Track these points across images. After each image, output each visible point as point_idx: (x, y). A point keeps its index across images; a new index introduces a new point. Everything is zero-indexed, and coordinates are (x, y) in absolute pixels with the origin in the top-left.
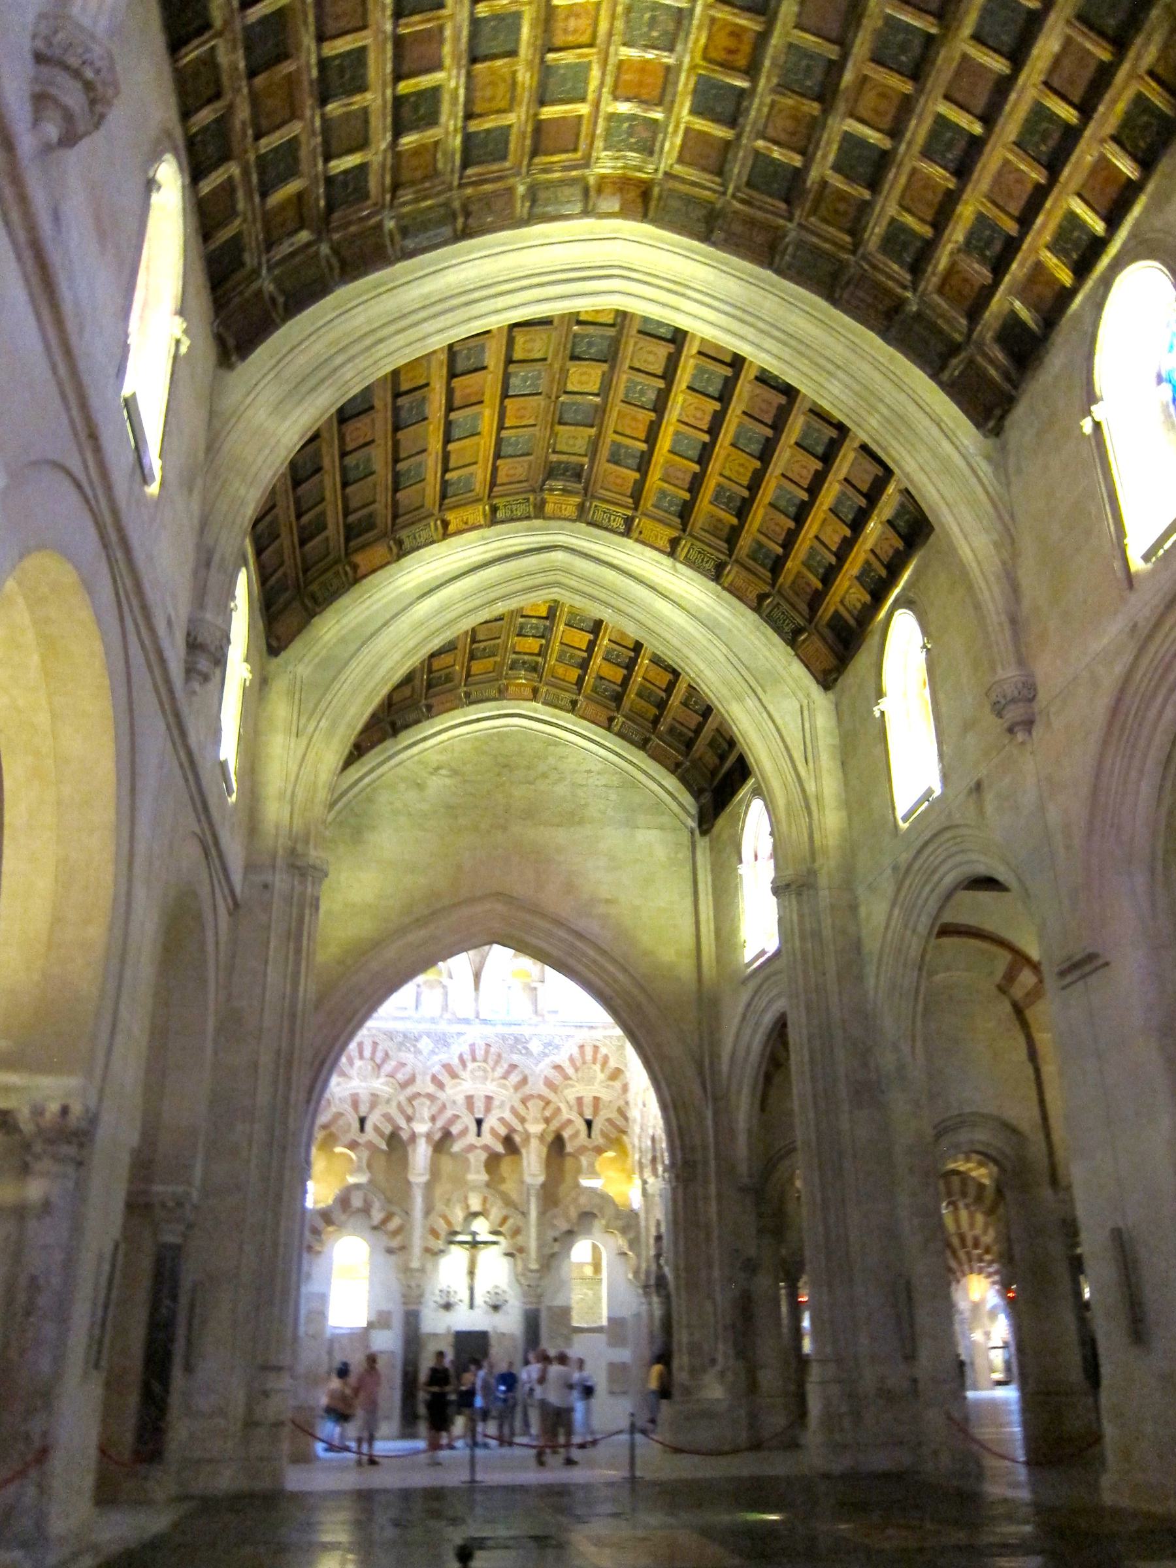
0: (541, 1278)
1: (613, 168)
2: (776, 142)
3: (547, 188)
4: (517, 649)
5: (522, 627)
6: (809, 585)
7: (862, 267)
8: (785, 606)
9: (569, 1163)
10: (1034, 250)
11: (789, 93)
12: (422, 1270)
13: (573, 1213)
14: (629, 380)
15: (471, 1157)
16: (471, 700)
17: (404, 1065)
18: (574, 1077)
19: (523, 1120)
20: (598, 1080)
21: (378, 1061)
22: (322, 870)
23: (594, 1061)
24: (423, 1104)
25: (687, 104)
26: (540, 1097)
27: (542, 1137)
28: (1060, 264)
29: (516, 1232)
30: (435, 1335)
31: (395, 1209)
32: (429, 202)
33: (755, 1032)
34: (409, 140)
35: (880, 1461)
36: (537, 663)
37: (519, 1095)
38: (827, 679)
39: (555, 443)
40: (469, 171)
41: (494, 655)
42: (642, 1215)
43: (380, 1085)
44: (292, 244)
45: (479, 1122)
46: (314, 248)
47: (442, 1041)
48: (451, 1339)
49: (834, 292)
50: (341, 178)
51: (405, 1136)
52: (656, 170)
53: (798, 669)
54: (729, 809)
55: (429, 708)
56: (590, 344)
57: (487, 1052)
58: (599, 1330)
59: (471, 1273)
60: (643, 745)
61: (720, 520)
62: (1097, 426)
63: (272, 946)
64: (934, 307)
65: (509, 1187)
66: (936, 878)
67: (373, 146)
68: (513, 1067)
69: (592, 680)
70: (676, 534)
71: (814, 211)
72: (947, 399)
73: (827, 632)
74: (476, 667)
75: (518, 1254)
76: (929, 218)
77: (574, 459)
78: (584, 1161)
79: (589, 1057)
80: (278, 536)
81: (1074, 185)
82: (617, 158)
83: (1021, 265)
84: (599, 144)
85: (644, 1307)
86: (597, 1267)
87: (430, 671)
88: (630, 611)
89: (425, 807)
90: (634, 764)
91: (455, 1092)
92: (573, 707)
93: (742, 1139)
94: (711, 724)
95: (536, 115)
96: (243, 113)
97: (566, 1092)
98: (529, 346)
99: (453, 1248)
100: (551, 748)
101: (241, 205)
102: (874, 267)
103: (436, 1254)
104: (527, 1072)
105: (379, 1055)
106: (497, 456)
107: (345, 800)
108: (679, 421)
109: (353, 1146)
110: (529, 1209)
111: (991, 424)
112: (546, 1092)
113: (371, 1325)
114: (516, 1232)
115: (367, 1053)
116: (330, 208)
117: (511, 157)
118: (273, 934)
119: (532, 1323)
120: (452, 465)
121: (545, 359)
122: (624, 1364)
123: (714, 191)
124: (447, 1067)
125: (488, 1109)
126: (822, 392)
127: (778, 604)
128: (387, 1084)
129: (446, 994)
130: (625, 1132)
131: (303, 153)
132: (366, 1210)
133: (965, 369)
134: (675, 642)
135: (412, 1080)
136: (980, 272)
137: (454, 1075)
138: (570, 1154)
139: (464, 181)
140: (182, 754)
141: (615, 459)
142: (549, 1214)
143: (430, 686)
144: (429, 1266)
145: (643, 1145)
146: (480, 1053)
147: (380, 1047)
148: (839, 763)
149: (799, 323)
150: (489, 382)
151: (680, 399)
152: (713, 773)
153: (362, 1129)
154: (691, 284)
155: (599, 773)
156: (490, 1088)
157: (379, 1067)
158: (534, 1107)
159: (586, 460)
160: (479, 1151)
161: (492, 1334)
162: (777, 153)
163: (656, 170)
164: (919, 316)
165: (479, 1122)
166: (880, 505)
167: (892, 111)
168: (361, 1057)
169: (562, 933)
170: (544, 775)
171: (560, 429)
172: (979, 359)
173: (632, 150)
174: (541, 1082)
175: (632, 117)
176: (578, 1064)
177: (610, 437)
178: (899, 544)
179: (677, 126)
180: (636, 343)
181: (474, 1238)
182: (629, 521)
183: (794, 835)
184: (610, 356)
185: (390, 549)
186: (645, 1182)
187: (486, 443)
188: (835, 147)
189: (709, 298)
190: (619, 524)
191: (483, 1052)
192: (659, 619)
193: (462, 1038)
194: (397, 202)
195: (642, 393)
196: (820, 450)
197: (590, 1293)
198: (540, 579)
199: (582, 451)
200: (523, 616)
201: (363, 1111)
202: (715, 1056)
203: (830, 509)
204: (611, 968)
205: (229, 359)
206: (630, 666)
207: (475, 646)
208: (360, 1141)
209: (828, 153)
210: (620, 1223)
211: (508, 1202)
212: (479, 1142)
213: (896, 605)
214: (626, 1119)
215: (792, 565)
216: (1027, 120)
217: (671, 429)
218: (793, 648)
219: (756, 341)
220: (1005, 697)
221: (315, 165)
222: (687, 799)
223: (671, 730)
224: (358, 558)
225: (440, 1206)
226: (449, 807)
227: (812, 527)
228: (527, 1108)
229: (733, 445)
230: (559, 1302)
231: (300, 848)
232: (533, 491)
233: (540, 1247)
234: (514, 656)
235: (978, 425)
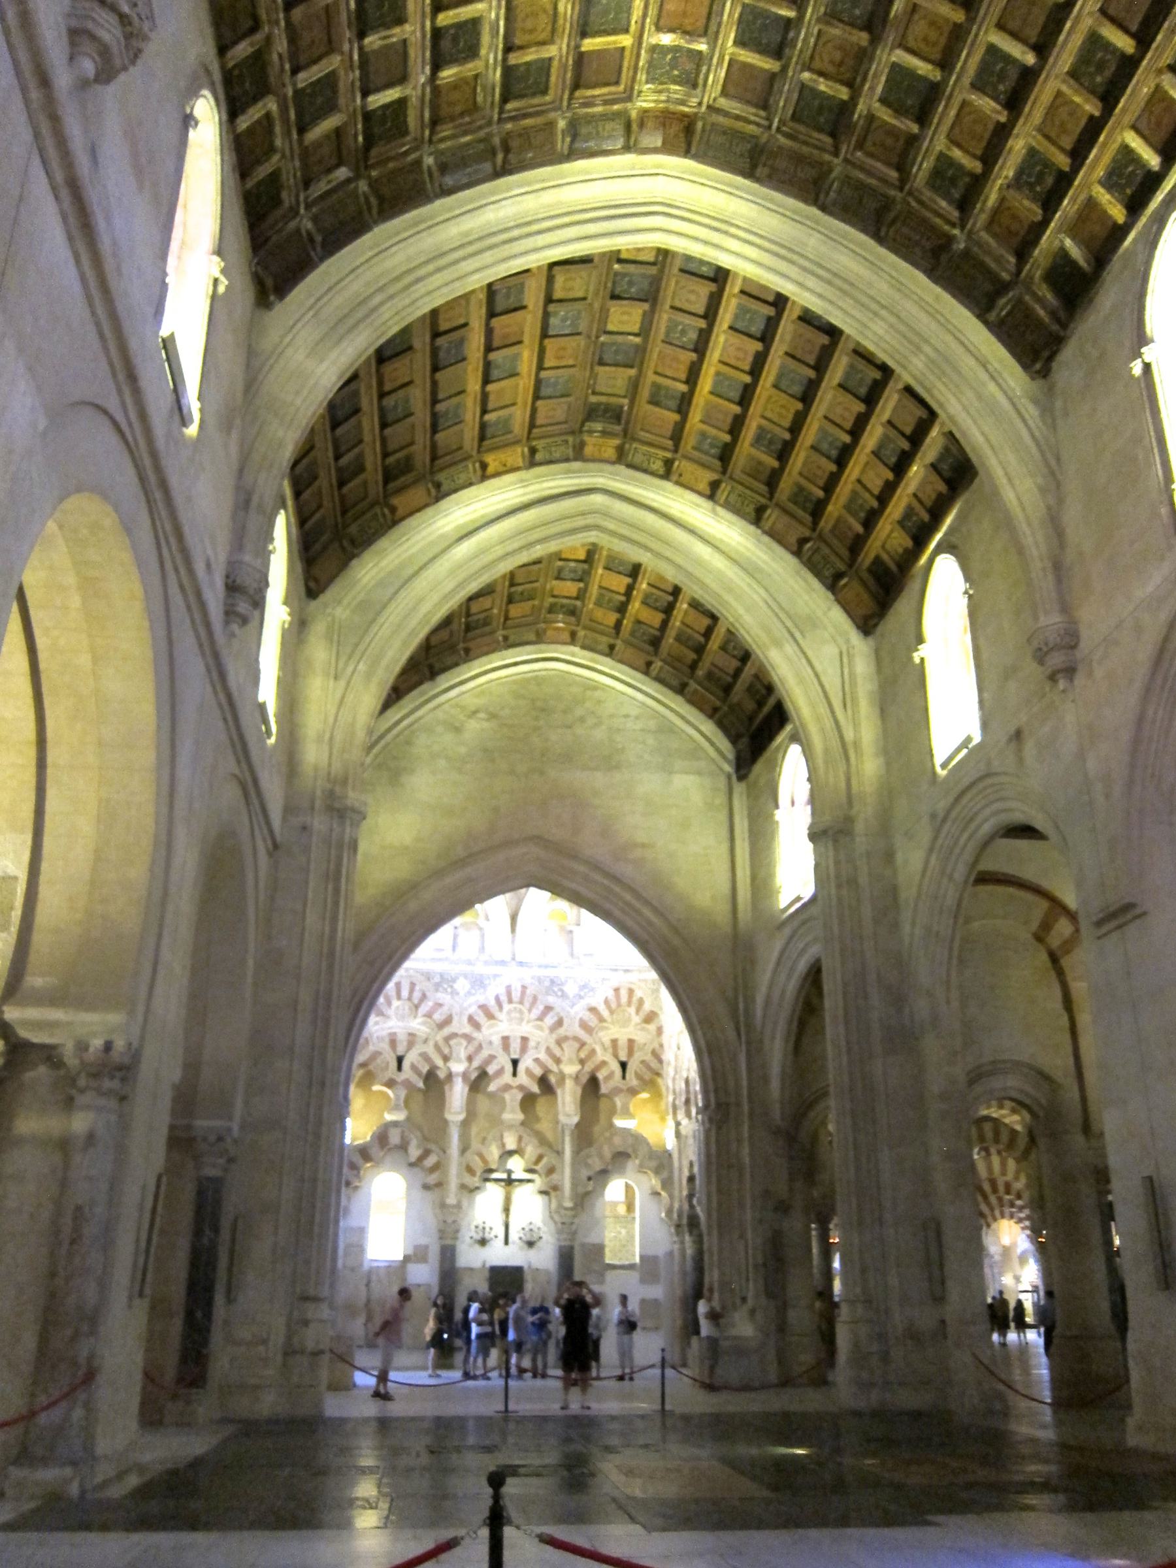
0: (575, 1216)
1: (655, 101)
2: (821, 74)
3: (589, 122)
4: (556, 593)
5: (560, 570)
6: (850, 528)
7: (908, 204)
8: (826, 550)
9: (603, 1104)
10: (1086, 185)
11: (835, 22)
12: (459, 1206)
13: (607, 1153)
14: (670, 320)
15: (507, 1096)
16: (508, 644)
17: (441, 1005)
18: (609, 1020)
19: (558, 1061)
20: (633, 1023)
21: (416, 1001)
22: (360, 812)
23: (629, 1003)
24: (461, 1044)
25: (732, 35)
26: (576, 1039)
27: (577, 1078)
28: (1113, 200)
29: (551, 1171)
30: (471, 1269)
31: (433, 1147)
32: (468, 138)
33: (789, 977)
34: (448, 74)
35: (908, 1399)
36: (575, 607)
37: (554, 1036)
38: (867, 625)
39: (595, 383)
40: (509, 106)
41: (533, 599)
42: (675, 1156)
43: (418, 1025)
44: (329, 182)
45: (515, 1063)
46: (352, 186)
47: (479, 982)
48: (487, 1274)
49: (879, 230)
50: (380, 113)
51: (442, 1074)
52: (700, 104)
53: (837, 615)
54: (767, 754)
55: (467, 651)
56: (631, 283)
57: (523, 993)
58: (631, 1267)
59: (507, 1210)
60: (680, 690)
61: (760, 463)
62: (1147, 367)
63: (312, 884)
64: (980, 244)
65: (544, 1126)
66: (973, 826)
67: (412, 82)
68: (548, 1009)
69: (630, 625)
70: (715, 476)
71: (860, 145)
72: (993, 339)
73: (865, 575)
74: (515, 611)
75: (553, 1194)
76: (979, 152)
77: (613, 400)
78: (618, 1101)
79: (624, 1000)
80: (315, 478)
81: (1128, 119)
82: (660, 92)
83: (1074, 200)
84: (642, 76)
85: (676, 1246)
86: (630, 1207)
87: (468, 615)
88: (668, 554)
89: (463, 750)
90: (672, 710)
91: (492, 1033)
92: (610, 652)
93: (775, 1084)
94: (749, 671)
95: (578, 46)
96: (281, 45)
97: (601, 1034)
98: (570, 284)
99: (488, 1184)
100: (589, 693)
101: (278, 142)
102: (920, 202)
103: (473, 1190)
104: (562, 1014)
105: (417, 995)
106: (537, 397)
107: (383, 743)
108: (720, 362)
109: (390, 1084)
110: (563, 1148)
111: (1038, 366)
112: (582, 1034)
113: (407, 1259)
114: (551, 1171)
115: (405, 993)
116: (370, 141)
117: (551, 92)
118: (312, 876)
119: (566, 1258)
120: (491, 406)
121: (584, 299)
122: (656, 1300)
123: (758, 124)
124: (484, 1008)
126: (867, 332)
127: (818, 548)
128: (424, 1023)
129: (483, 936)
130: (658, 1074)
131: (342, 86)
132: (403, 1147)
133: (1013, 308)
134: (714, 586)
135: (448, 1021)
136: (1030, 209)
137: (490, 1016)
138: (604, 1095)
139: (504, 116)
140: (222, 696)
141: (654, 401)
142: (583, 1153)
143: (468, 628)
144: (465, 1204)
145: (677, 1088)
146: (516, 995)
147: (417, 988)
148: (878, 711)
149: (845, 262)
150: (529, 322)
151: (722, 339)
152: (751, 719)
153: (400, 1068)
154: (734, 221)
155: (637, 718)
156: (526, 1029)
157: (417, 1007)
158: (569, 1049)
159: (626, 401)
160: (515, 1091)
161: (526, 1267)
162: (823, 86)
163: (700, 104)
164: (966, 254)
165: (515, 1063)
166: (923, 448)
167: (943, 41)
168: (399, 997)
169: (598, 877)
170: (582, 719)
171: (601, 370)
172: (1027, 298)
173: (675, 83)
174: (577, 1025)
175: (676, 49)
176: (614, 1006)
177: (650, 377)
178: (942, 487)
179: (721, 58)
180: (677, 282)
181: (509, 1176)
182: (668, 464)
183: (831, 780)
184: (651, 296)
185: (428, 491)
186: (678, 1124)
187: (525, 383)
188: (883, 79)
189: (752, 236)
190: (658, 466)
191: (519, 994)
192: (699, 562)
194: (435, 138)
195: (683, 332)
196: (863, 391)
197: (624, 1231)
198: (580, 522)
199: (622, 393)
200: (561, 560)
201: (400, 1050)
202: (749, 1000)
203: (873, 452)
204: (647, 912)
205: (268, 297)
206: (669, 610)
207: (513, 589)
209: (877, 84)
210: (653, 1164)
211: (543, 1141)
212: (515, 1082)
213: (939, 550)
214: (660, 1061)
215: (834, 509)
216: (1081, 49)
217: (712, 371)
218: (833, 593)
219: (801, 280)
220: (1046, 644)
221: (354, 101)
222: (725, 744)
223: (710, 676)
224: (395, 501)
225: (475, 1145)
226: (485, 750)
227: (853, 470)
228: (562, 1049)
229: (776, 386)
230: (593, 1239)
231: (338, 789)
232: (573, 433)
233: (574, 1185)
234: (551, 600)
235: (1025, 367)
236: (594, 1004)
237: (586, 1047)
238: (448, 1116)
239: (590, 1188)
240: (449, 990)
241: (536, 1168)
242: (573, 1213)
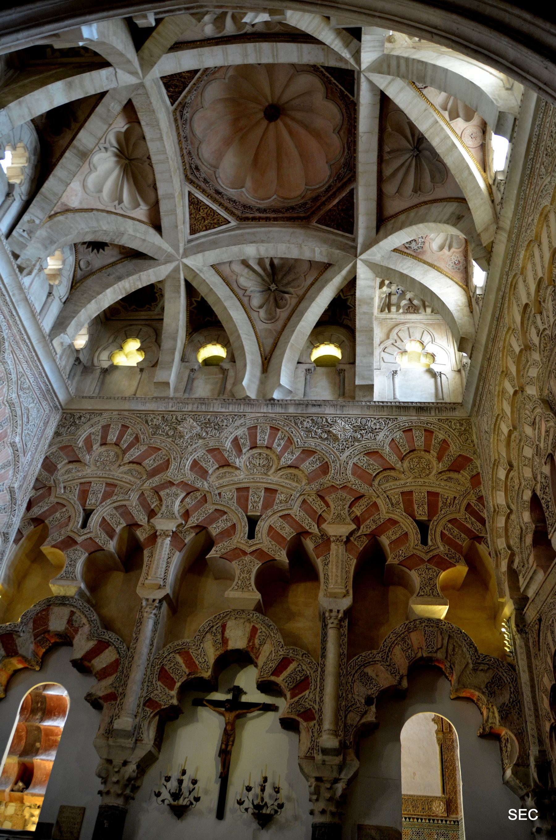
0: (341, 768)
18: (398, 466)
19: (320, 520)
20: (434, 472)
21: (125, 446)
37: (315, 486)
42: (522, 664)
45: (253, 522)
51: (141, 535)
57: (272, 437)
68: (308, 452)
105: (128, 439)
110: (324, 649)
115: (112, 437)
124: (215, 451)
125: (267, 505)
128: (130, 472)
130: (479, 539)
147: (129, 431)
153: (84, 525)
157: (124, 452)
165: (253, 522)
174: (349, 472)
193: (238, 423)
208: (79, 539)
210: (484, 678)
214: (483, 521)
228: (328, 505)
236: (373, 446)
237: (362, 502)
238: (141, 592)
239: (371, 717)
240: (171, 433)
241: (279, 680)
242: (337, 760)
